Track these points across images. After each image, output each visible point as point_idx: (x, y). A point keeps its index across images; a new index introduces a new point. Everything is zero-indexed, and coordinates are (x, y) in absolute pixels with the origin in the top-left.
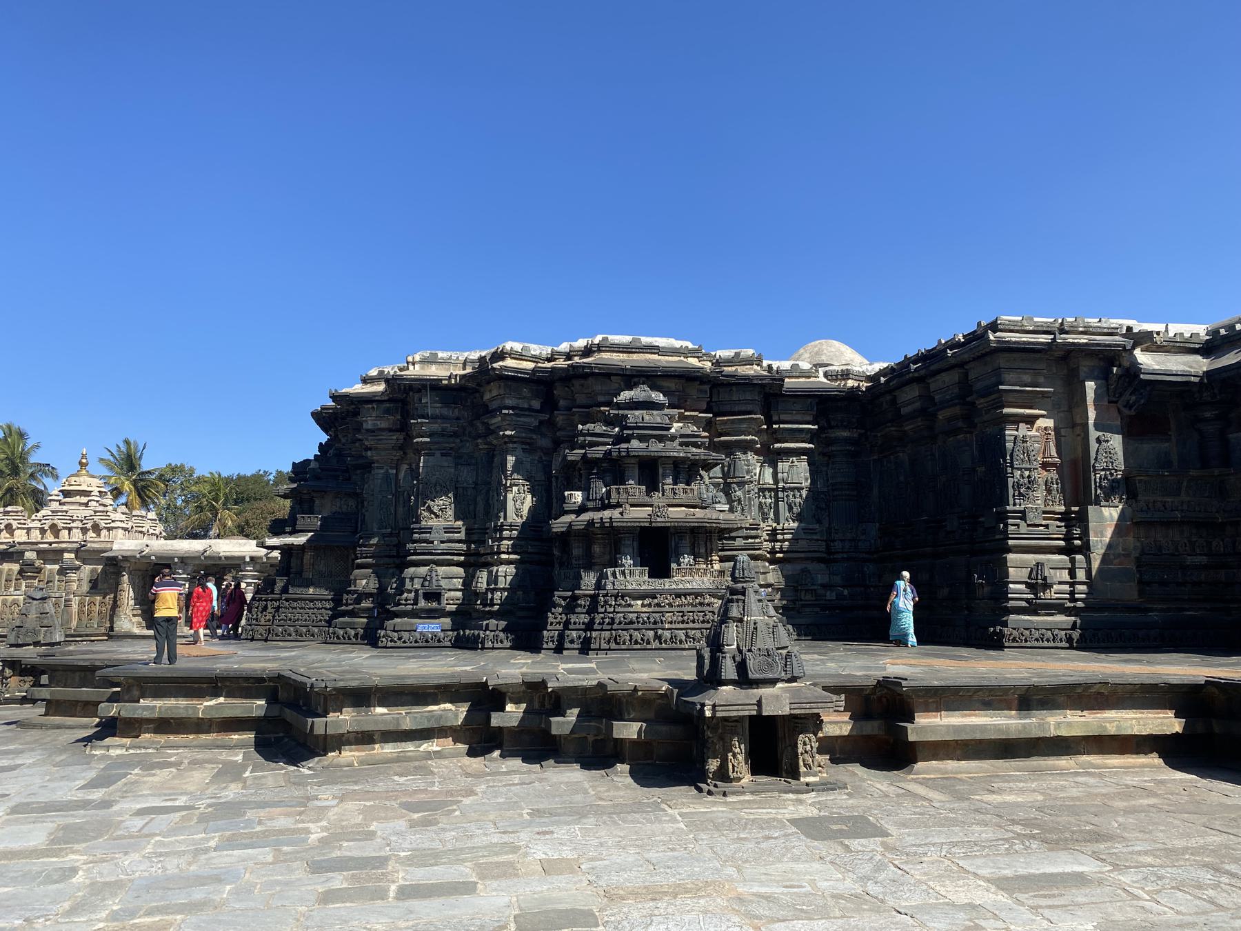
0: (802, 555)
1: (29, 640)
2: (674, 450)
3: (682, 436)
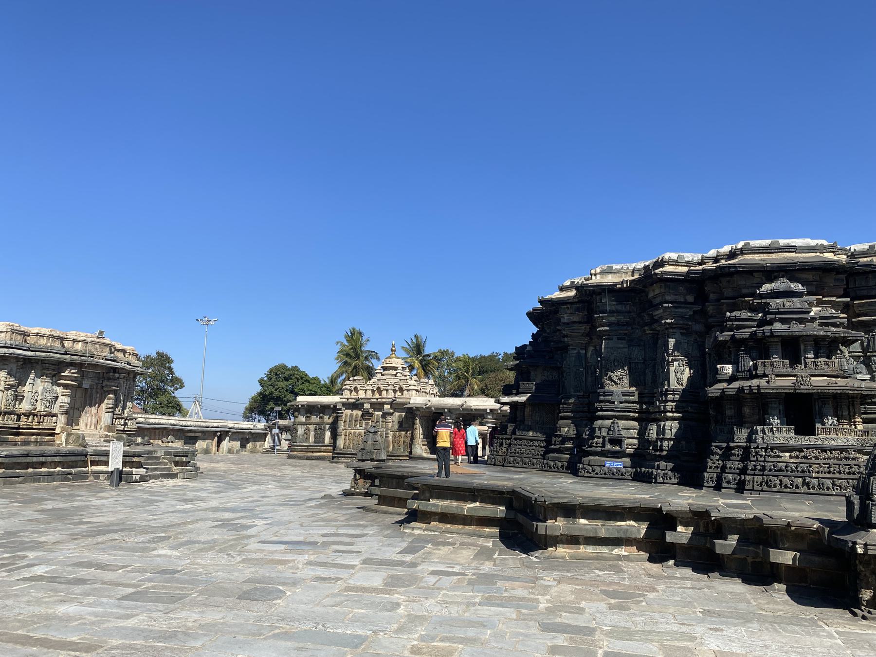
1: (368, 457)
2: (814, 330)
3: (821, 318)
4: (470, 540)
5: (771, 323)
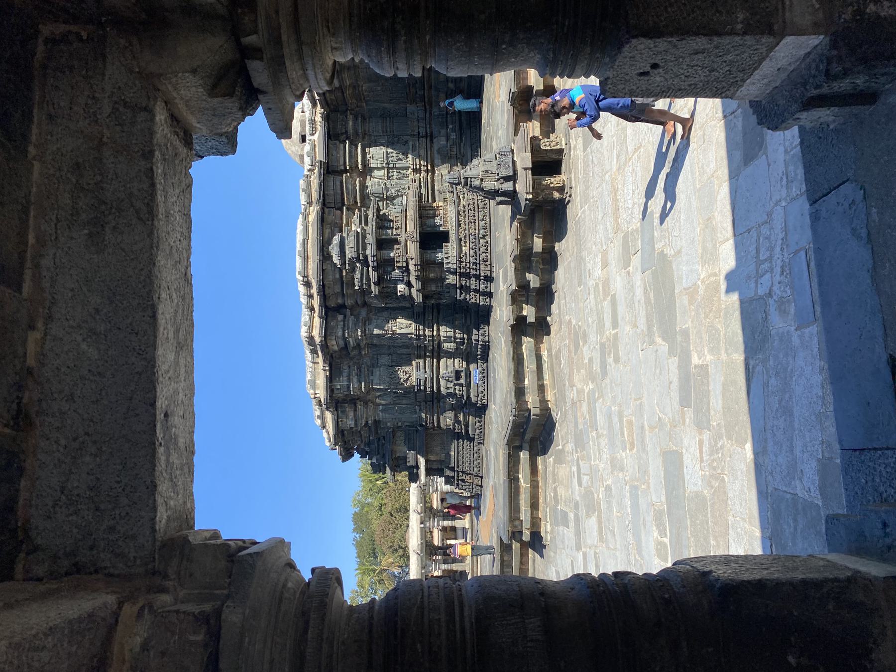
3: (360, 223)
5: (366, 257)
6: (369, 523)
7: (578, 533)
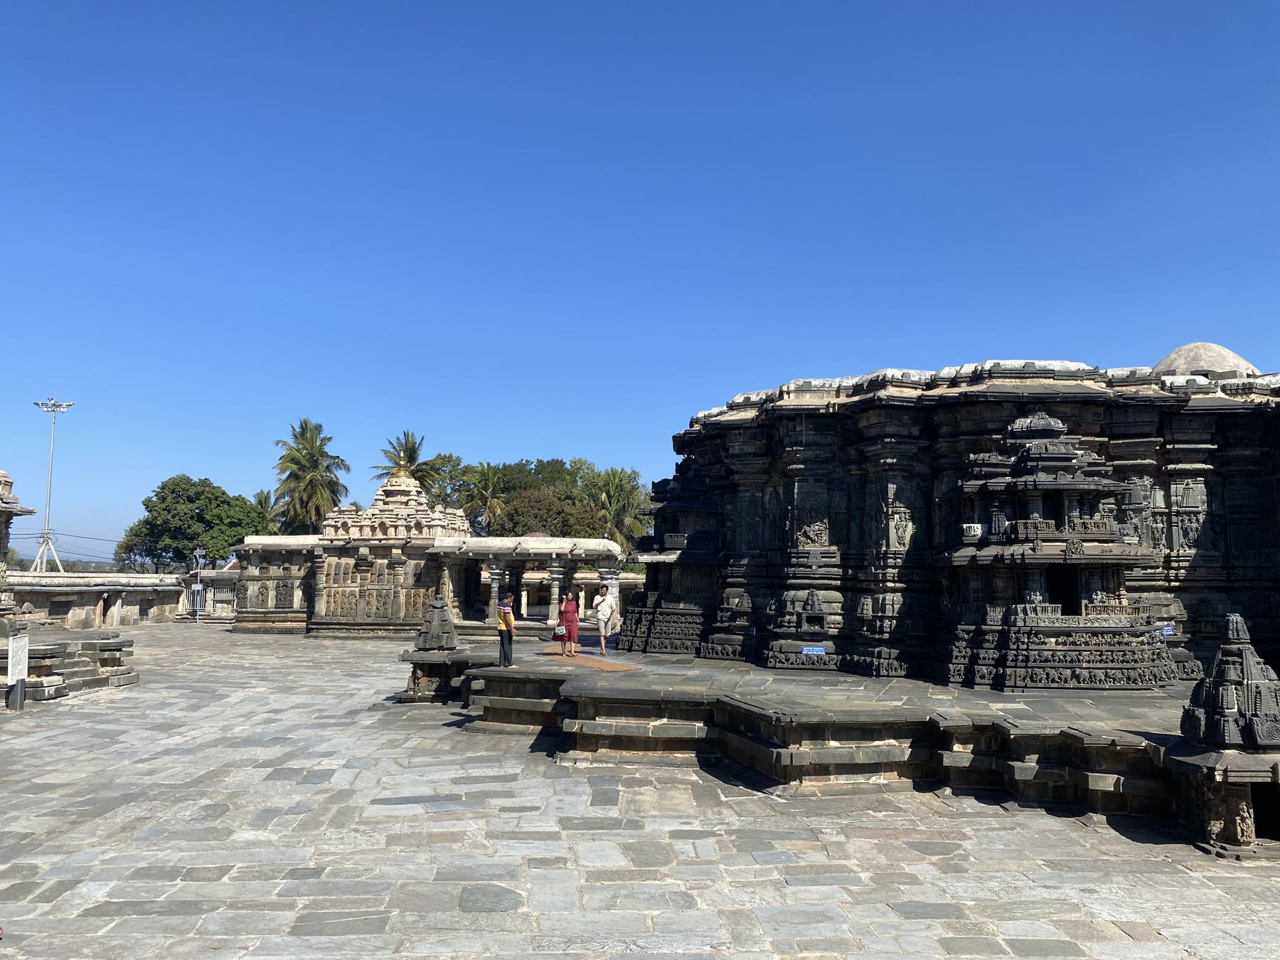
0: (1201, 584)
1: (435, 645)
3: (1090, 464)
4: (664, 772)
5: (1031, 472)
6: (551, 481)
7: (589, 824)
